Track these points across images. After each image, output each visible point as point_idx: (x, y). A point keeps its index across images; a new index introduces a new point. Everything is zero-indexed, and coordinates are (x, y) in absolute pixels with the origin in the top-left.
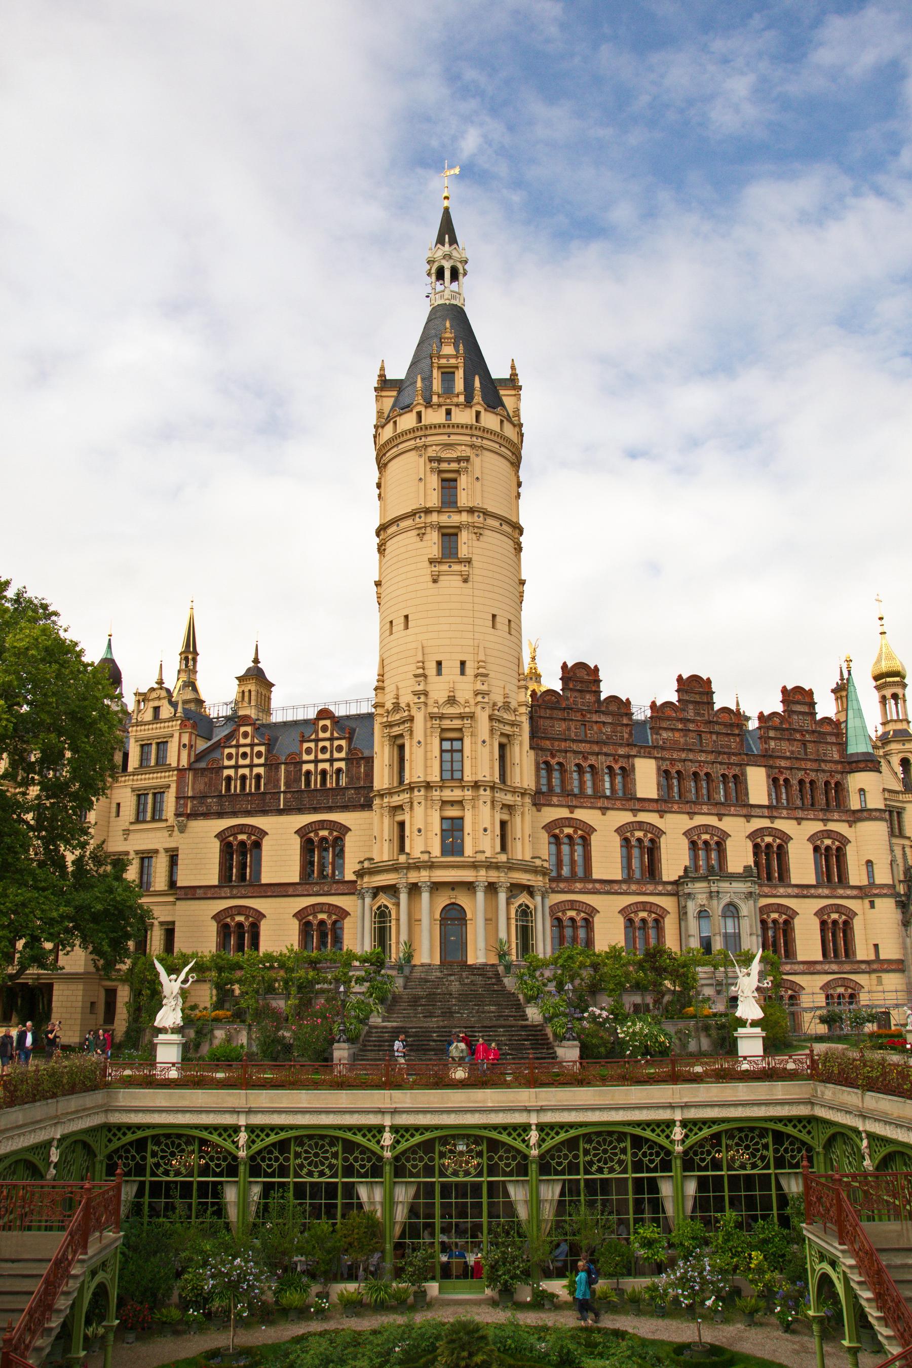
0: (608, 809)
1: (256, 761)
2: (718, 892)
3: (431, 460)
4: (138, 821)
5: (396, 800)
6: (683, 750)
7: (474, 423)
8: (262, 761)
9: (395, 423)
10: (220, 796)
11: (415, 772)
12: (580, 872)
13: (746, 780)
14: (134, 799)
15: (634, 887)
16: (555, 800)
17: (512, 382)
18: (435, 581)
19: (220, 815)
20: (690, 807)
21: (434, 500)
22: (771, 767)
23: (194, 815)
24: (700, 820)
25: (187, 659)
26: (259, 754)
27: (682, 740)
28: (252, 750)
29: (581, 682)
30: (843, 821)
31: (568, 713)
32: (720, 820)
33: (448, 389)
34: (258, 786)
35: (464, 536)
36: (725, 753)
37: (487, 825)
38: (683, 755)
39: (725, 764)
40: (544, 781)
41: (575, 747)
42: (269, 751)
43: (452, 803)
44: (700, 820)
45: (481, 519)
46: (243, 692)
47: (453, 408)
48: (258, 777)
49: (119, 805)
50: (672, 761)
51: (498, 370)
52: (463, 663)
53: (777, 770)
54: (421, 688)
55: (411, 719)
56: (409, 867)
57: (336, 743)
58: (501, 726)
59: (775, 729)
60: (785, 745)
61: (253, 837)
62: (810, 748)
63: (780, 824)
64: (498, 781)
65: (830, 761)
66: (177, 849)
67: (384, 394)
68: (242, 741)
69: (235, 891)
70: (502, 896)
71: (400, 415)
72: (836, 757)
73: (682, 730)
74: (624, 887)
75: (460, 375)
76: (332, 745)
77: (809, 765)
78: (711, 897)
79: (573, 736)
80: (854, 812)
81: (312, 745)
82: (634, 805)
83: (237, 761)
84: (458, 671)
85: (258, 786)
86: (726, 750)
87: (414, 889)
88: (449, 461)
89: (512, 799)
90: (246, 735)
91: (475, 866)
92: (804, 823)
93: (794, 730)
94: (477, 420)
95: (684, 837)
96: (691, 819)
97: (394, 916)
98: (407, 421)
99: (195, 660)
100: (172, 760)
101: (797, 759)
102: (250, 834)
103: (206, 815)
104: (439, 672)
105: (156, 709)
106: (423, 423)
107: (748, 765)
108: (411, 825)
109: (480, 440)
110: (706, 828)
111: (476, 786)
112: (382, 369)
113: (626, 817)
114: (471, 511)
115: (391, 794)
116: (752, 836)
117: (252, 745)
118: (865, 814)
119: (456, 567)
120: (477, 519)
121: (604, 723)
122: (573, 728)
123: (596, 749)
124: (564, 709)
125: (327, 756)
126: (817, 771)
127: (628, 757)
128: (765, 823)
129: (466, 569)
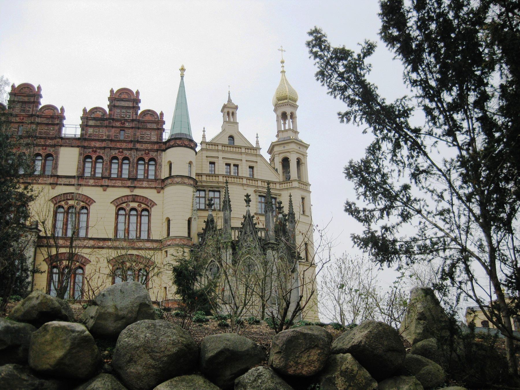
13: (57, 157)
22: (84, 147)
30: (151, 188)
53: (91, 150)
59: (95, 119)
65: (146, 143)
92: (109, 189)
101: (111, 141)
126: (131, 149)
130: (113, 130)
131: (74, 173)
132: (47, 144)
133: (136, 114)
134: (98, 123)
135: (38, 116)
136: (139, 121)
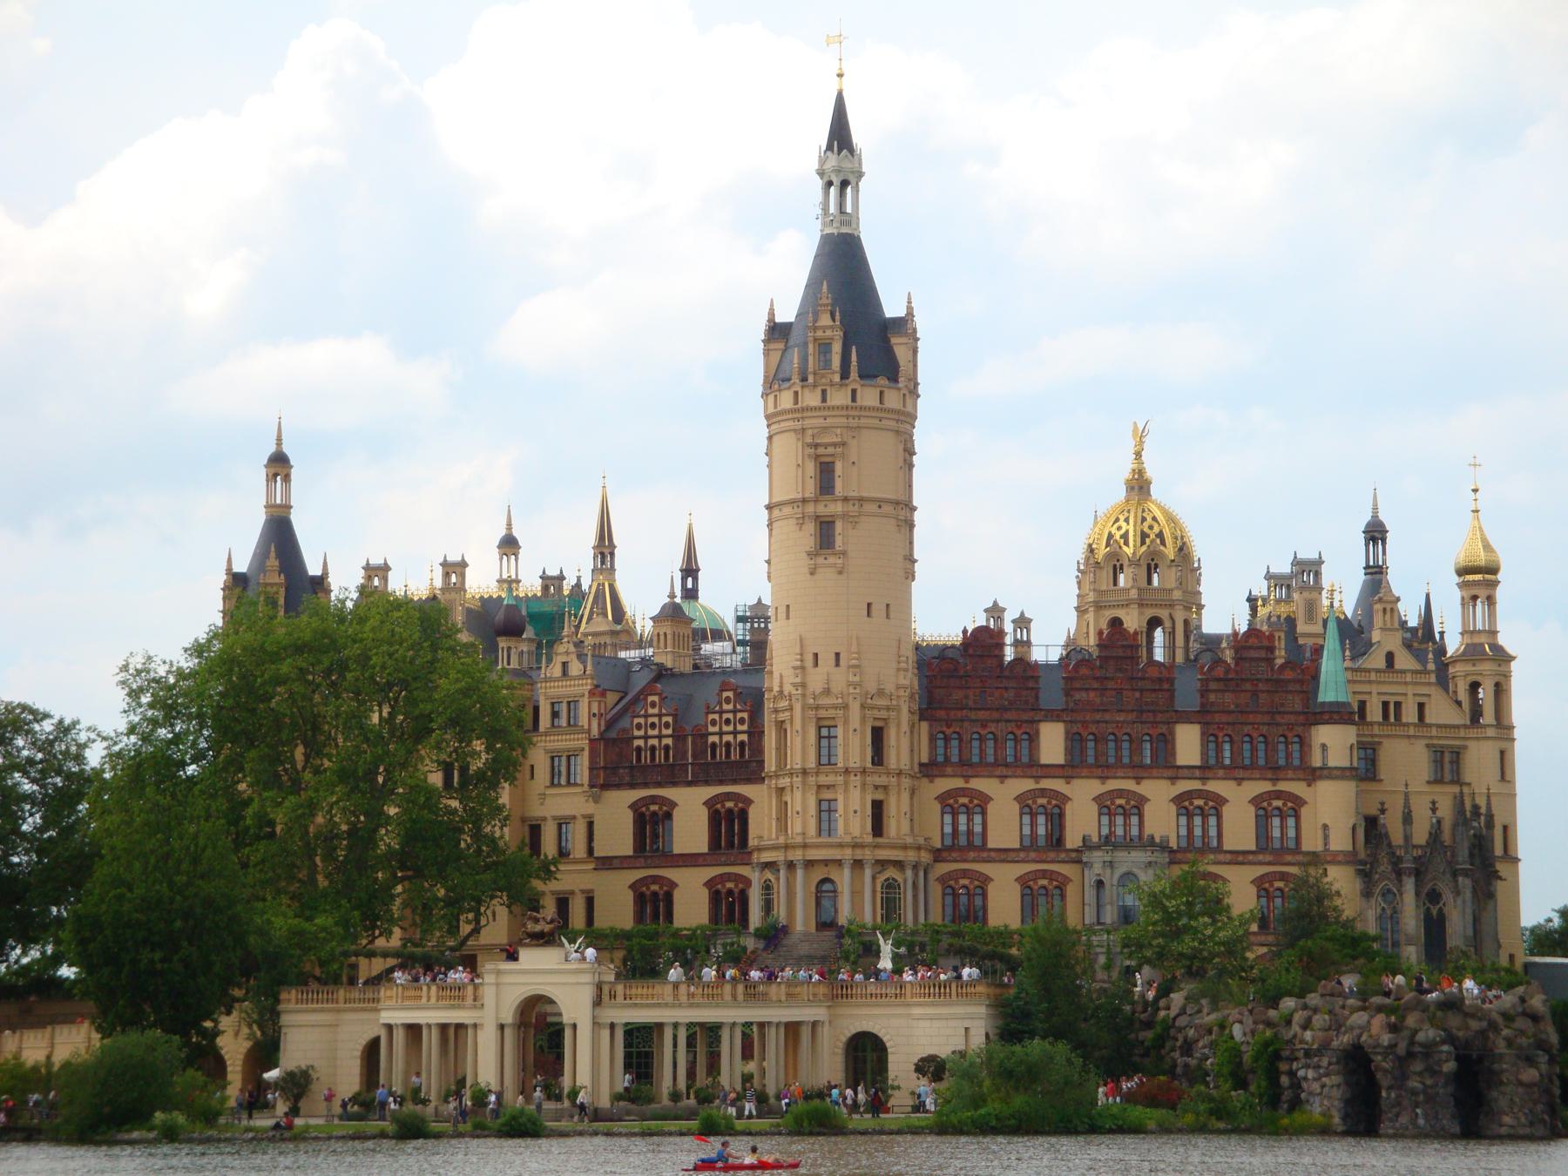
0: (1006, 777)
1: (665, 732)
2: (1111, 862)
3: (810, 445)
4: (552, 784)
5: (784, 782)
6: (1098, 711)
7: (850, 403)
8: (669, 732)
9: (776, 396)
10: (632, 768)
11: (795, 760)
12: (978, 841)
14: (548, 761)
15: (1033, 855)
16: (949, 770)
17: (903, 325)
18: (812, 574)
19: (632, 786)
20: (1103, 770)
21: (810, 490)
22: (1208, 723)
23: (606, 786)
24: (1113, 785)
25: (602, 554)
26: (667, 725)
27: (1098, 700)
28: (660, 720)
29: (982, 646)
31: (966, 681)
32: (1138, 783)
33: (827, 364)
34: (667, 757)
35: (839, 526)
36: (1149, 711)
37: (858, 808)
38: (1098, 717)
39: (1149, 722)
40: (941, 751)
41: (973, 715)
42: (675, 721)
43: (828, 787)
44: (1113, 785)
45: (856, 506)
46: (658, 634)
47: (828, 389)
48: (667, 748)
49: (532, 767)
50: (1085, 724)
51: (892, 308)
52: (837, 655)
53: (1216, 726)
54: (798, 680)
55: (791, 709)
56: (787, 847)
57: (739, 715)
58: (876, 712)
60: (1228, 697)
61: (665, 808)
62: (1263, 697)
63: (1214, 786)
64: (870, 765)
65: (1288, 713)
66: (590, 816)
67: (772, 346)
68: (651, 711)
69: (649, 861)
70: (868, 873)
71: (780, 390)
72: (1298, 707)
73: (1096, 689)
74: (1022, 855)
75: (837, 348)
76: (735, 717)
77: (1259, 718)
78: (1104, 866)
79: (971, 703)
80: (1314, 769)
81: (716, 717)
82: (1037, 771)
83: (646, 732)
84: (833, 662)
85: (667, 757)
86: (1152, 708)
87: (791, 866)
88: (826, 446)
89: (887, 780)
90: (653, 705)
91: (841, 846)
92: (1246, 784)
93: (1242, 680)
94: (854, 399)
95: (1094, 803)
96: (1103, 784)
97: (775, 890)
98: (786, 400)
99: (612, 554)
100: (583, 720)
101: (1242, 712)
102: (662, 805)
103: (618, 786)
104: (816, 664)
105: (565, 664)
106: (800, 405)
107: (1176, 722)
108: (792, 806)
109: (856, 421)
110: (1120, 793)
111: (847, 771)
112: (772, 313)
113: (1028, 785)
114: (846, 499)
115: (777, 776)
116: (1179, 800)
117: (660, 716)
118: (1325, 772)
119: (832, 560)
120: (852, 509)
121: (1006, 688)
122: (972, 697)
123: (996, 715)
124: (961, 677)
125: (730, 728)
127: (1032, 722)
128: (1195, 785)
129: (840, 561)
130: (1242, 695)
131: (1198, 762)
132: (1158, 719)
133: (1272, 670)
134: (1221, 686)
135: (1142, 679)
136: (1278, 681)
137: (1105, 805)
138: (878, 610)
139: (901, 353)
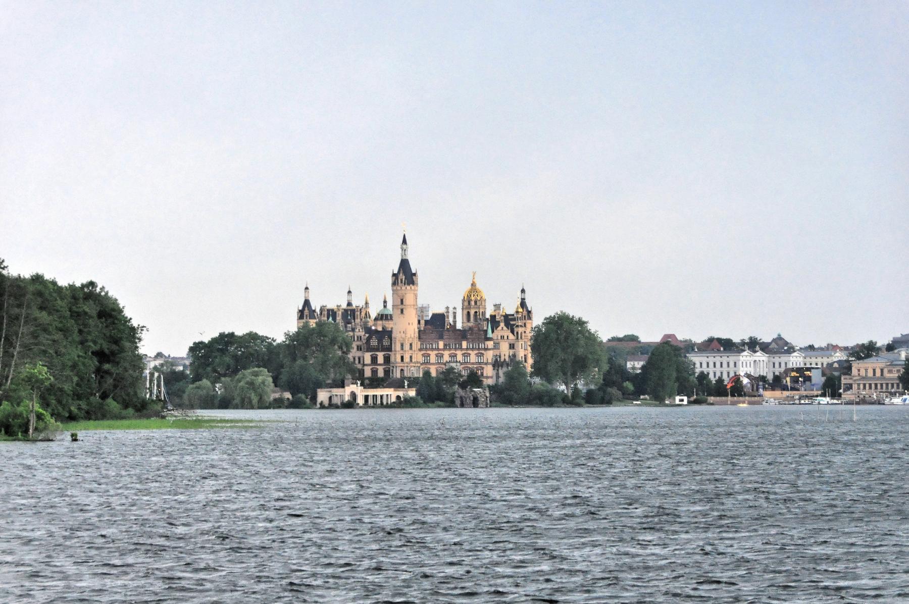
17: (415, 274)
19: (370, 352)
20: (450, 349)
63: (469, 352)
98: (395, 288)
113: (437, 352)
116: (463, 354)
137: (450, 356)
138: (411, 324)
139: (414, 279)
